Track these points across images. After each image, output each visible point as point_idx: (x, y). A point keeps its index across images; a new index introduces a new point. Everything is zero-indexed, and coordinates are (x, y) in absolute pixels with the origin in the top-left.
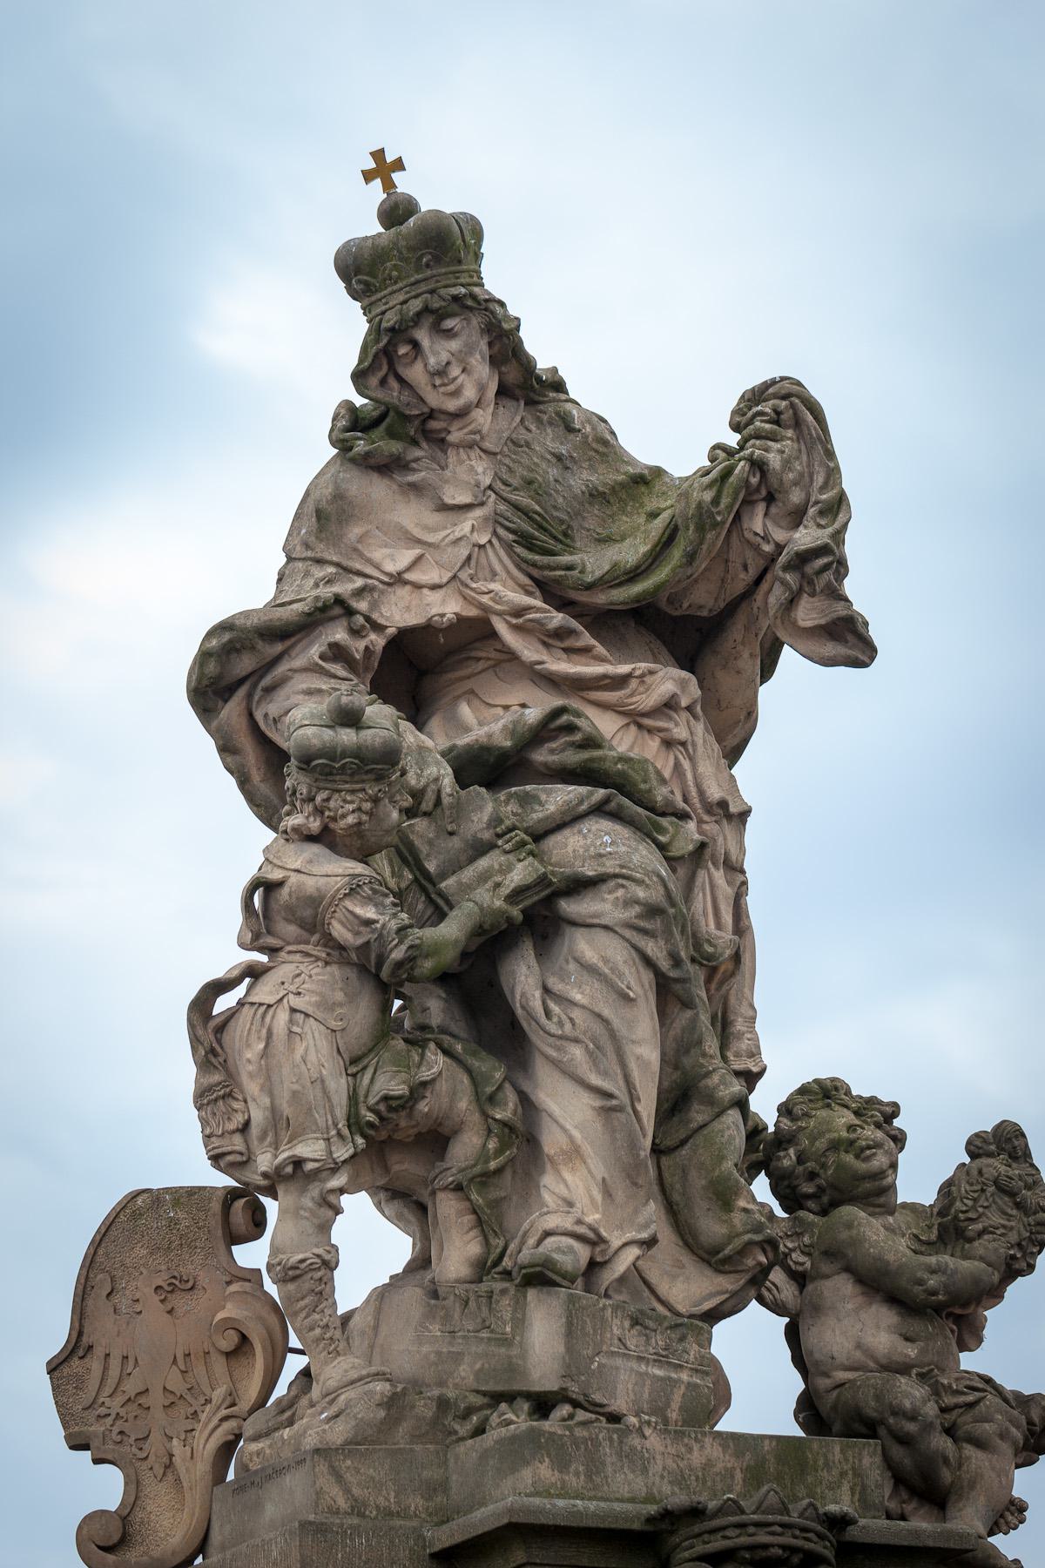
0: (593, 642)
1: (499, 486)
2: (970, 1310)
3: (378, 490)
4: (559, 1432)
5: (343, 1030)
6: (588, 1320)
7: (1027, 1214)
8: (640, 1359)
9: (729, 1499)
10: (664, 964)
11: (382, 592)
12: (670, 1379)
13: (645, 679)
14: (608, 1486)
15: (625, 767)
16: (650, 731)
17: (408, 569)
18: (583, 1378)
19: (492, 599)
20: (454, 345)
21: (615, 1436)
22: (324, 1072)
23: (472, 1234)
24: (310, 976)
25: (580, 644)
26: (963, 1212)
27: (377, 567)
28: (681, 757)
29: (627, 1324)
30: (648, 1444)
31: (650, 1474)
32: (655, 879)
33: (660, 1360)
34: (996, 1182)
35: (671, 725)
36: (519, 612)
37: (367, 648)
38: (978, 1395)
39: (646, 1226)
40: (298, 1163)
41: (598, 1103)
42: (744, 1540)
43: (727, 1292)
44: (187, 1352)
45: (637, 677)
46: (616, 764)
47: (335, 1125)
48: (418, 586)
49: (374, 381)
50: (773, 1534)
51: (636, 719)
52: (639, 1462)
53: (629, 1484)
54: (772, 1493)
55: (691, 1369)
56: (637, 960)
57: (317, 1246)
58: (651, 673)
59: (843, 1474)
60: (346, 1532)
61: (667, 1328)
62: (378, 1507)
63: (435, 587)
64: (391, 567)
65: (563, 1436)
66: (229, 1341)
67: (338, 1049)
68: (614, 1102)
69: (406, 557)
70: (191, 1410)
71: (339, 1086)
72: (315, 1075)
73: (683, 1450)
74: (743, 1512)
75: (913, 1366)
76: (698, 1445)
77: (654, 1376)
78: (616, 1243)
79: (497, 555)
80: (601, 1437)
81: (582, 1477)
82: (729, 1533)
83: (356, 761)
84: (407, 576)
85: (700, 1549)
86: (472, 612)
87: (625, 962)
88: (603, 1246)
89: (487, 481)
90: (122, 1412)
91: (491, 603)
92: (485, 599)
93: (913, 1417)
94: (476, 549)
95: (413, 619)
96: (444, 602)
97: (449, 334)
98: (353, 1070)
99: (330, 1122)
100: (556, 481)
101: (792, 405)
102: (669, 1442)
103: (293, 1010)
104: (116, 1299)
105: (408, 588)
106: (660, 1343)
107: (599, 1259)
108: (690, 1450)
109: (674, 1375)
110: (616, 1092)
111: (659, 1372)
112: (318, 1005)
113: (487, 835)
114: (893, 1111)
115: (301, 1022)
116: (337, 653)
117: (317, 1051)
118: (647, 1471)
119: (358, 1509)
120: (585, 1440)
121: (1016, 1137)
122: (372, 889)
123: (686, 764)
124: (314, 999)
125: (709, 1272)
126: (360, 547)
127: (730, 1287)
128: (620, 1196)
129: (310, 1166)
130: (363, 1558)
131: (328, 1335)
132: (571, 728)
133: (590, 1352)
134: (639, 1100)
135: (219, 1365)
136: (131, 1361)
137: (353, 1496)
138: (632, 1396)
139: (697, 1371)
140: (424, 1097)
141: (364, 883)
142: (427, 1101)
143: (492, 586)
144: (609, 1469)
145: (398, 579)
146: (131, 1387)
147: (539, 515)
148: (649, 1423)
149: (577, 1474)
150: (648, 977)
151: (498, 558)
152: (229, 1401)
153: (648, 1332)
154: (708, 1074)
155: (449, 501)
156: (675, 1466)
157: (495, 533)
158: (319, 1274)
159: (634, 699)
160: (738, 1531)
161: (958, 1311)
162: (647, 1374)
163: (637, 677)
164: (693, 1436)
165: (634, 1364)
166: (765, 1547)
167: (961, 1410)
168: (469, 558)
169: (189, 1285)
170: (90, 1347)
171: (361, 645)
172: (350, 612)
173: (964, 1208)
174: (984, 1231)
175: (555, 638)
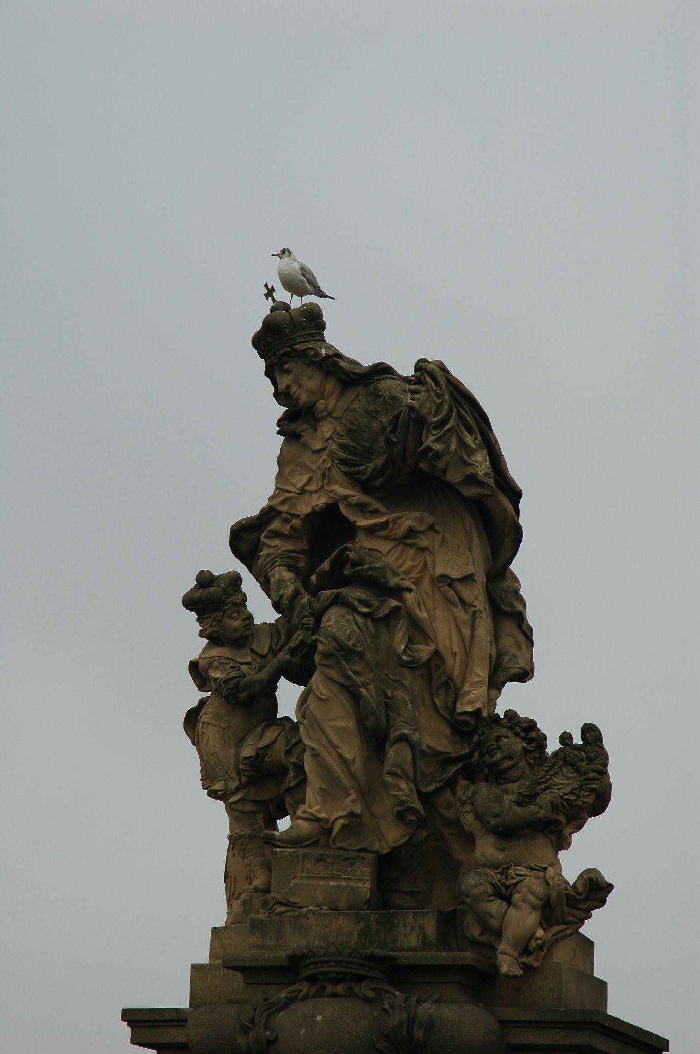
2: (560, 828)
5: (228, 727)
10: (341, 680)
13: (397, 522)
15: (372, 573)
16: (411, 545)
20: (290, 377)
24: (212, 705)
32: (329, 639)
35: (417, 541)
39: (344, 809)
42: (317, 970)
46: (368, 571)
48: (311, 493)
50: (330, 966)
54: (332, 946)
58: (400, 518)
59: (413, 929)
63: (316, 492)
64: (299, 485)
68: (316, 752)
69: (305, 478)
75: (502, 864)
78: (333, 818)
81: (273, 941)
82: (311, 967)
83: (201, 605)
85: (304, 975)
86: (331, 501)
89: (328, 435)
91: (334, 496)
92: (331, 495)
95: (309, 510)
96: (319, 498)
97: (288, 372)
103: (204, 722)
105: (308, 494)
116: (276, 534)
121: (589, 732)
122: (219, 663)
123: (429, 561)
126: (288, 477)
130: (220, 980)
131: (252, 868)
134: (338, 747)
145: (303, 491)
147: (353, 447)
150: (334, 687)
151: (336, 474)
153: (327, 864)
155: (314, 449)
156: (322, 931)
158: (240, 842)
163: (392, 522)
164: (333, 916)
166: (328, 973)
171: (288, 527)
172: (280, 513)
174: (547, 788)
175: (361, 508)
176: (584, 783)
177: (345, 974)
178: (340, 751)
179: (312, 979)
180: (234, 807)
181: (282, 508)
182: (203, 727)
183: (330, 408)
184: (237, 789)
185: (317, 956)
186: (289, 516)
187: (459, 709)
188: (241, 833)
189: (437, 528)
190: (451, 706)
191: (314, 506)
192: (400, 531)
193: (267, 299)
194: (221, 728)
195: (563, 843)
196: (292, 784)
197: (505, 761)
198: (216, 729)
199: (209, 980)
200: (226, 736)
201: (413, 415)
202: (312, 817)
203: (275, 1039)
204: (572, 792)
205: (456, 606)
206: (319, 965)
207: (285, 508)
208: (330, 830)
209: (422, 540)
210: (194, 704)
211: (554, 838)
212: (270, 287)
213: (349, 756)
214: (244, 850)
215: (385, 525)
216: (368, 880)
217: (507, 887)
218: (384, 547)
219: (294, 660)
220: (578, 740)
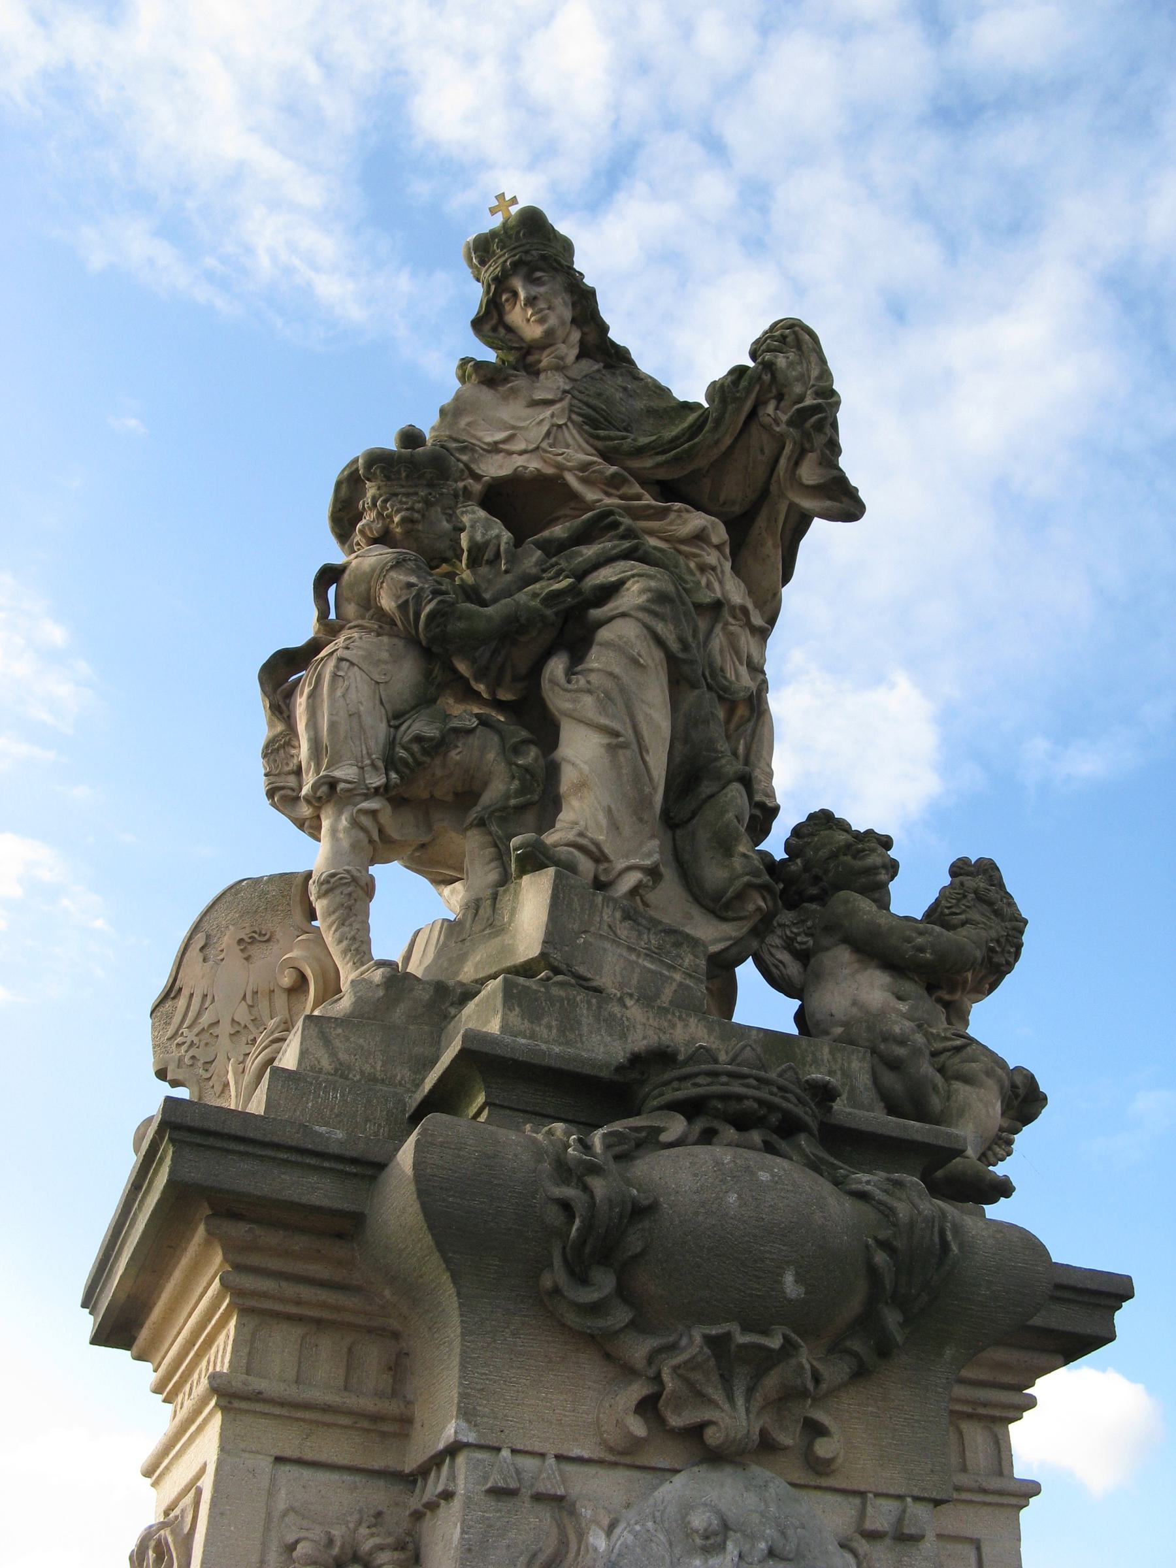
2: (957, 996)
4: (534, 987)
5: (386, 683)
6: (576, 900)
8: (631, 949)
9: (701, 1047)
10: (674, 646)
11: (482, 455)
12: (661, 974)
14: (582, 1043)
17: (504, 441)
18: (567, 949)
19: (565, 459)
22: (362, 708)
23: (493, 864)
26: (949, 908)
27: (480, 440)
28: (711, 577)
29: (618, 915)
30: (628, 1013)
31: (629, 1040)
33: (650, 955)
36: (584, 467)
39: (649, 855)
41: (606, 740)
42: (716, 1089)
43: (730, 938)
44: (255, 990)
45: (675, 511)
47: (369, 755)
48: (510, 453)
49: (487, 328)
50: (748, 1086)
52: (622, 1030)
53: (606, 1046)
54: (749, 1048)
55: (684, 972)
56: (648, 637)
57: (348, 865)
58: (687, 511)
60: (320, 1084)
61: (661, 931)
62: (362, 1073)
64: (489, 439)
65: (537, 991)
66: (287, 980)
67: (381, 700)
70: (251, 1037)
71: (379, 730)
72: (353, 710)
73: (666, 1024)
74: (716, 1061)
76: (683, 1023)
77: (645, 967)
78: (620, 865)
79: (571, 434)
80: (578, 999)
81: (554, 1031)
82: (700, 1080)
84: (502, 446)
85: (670, 1096)
86: (550, 471)
87: (637, 637)
88: (606, 865)
90: (196, 1040)
92: (559, 458)
93: (902, 1041)
94: (555, 428)
98: (397, 723)
99: (364, 752)
100: (621, 399)
101: (795, 333)
102: (651, 1015)
104: (207, 951)
105: (502, 454)
106: (653, 941)
107: (603, 878)
108: (674, 1026)
112: (365, 658)
113: (534, 571)
115: (346, 669)
117: (357, 691)
118: (626, 1038)
119: (341, 1070)
120: (561, 1000)
124: (361, 653)
125: (715, 922)
127: (734, 934)
128: (627, 831)
133: (576, 927)
135: (281, 1000)
136: (209, 999)
137: (338, 1059)
138: (619, 978)
139: (691, 976)
140: (457, 747)
141: (410, 560)
142: (459, 750)
144: (585, 1029)
145: (495, 448)
146: (205, 1020)
147: (605, 411)
149: (549, 1027)
150: (659, 655)
151: (572, 435)
152: (283, 1027)
153: (640, 928)
154: (717, 759)
157: (570, 419)
159: (673, 528)
160: (709, 1080)
162: (637, 963)
163: (675, 511)
166: (740, 1098)
167: (948, 1054)
168: (548, 434)
169: (265, 938)
170: (180, 989)
173: (949, 905)
175: (613, 484)
177: (771, 1107)
179: (691, 1108)
182: (337, 667)
186: (467, 473)
188: (355, 873)
191: (519, 467)
194: (372, 679)
196: (513, 802)
198: (365, 676)
199: (310, 1104)
202: (593, 848)
205: (741, 664)
207: (465, 458)
209: (709, 554)
219: (548, 612)
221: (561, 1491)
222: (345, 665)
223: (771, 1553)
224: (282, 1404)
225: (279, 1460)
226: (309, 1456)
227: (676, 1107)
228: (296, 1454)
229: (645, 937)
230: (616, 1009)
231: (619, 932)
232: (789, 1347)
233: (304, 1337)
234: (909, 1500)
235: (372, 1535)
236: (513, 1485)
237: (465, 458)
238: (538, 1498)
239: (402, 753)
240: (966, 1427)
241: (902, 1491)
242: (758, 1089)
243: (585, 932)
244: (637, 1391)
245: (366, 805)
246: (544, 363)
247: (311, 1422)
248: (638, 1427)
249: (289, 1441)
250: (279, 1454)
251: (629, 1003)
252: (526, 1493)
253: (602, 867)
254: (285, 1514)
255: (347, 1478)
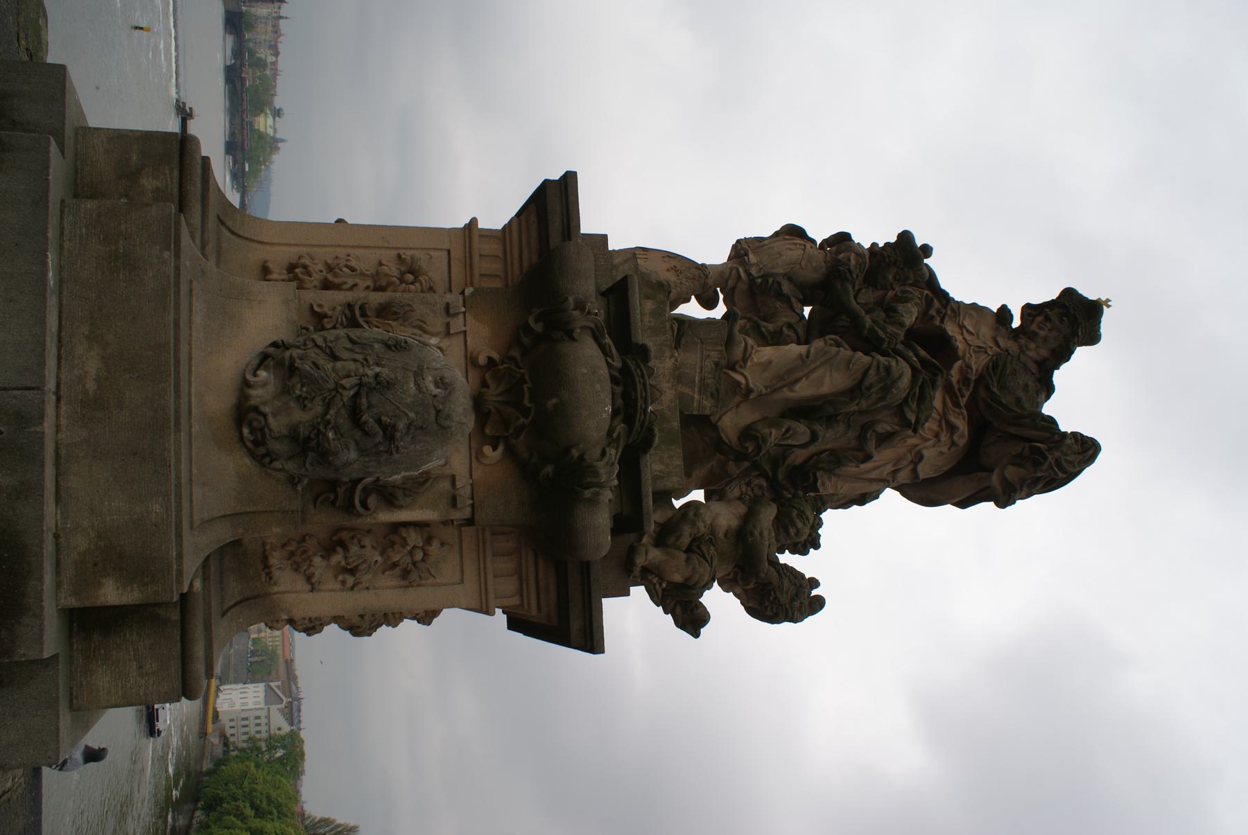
0: (967, 396)
1: (1010, 358)
2: (741, 583)
3: (991, 320)
5: (802, 268)
7: (789, 603)
8: (701, 368)
10: (867, 382)
12: (695, 386)
16: (940, 426)
20: (1057, 323)
21: (668, 343)
22: (784, 257)
25: (965, 392)
27: (964, 319)
28: (933, 441)
29: (716, 359)
30: (667, 360)
33: (702, 380)
34: (801, 586)
35: (945, 433)
36: (969, 367)
37: (934, 316)
38: (710, 560)
39: (755, 385)
40: (746, 254)
43: (731, 443)
47: (765, 266)
48: (962, 334)
49: (1029, 311)
51: (944, 416)
55: (700, 401)
58: (964, 418)
63: (965, 339)
64: (965, 323)
73: (667, 378)
74: (649, 378)
77: (695, 377)
78: (745, 373)
79: (986, 358)
80: (667, 335)
82: (638, 371)
86: (960, 353)
88: (743, 365)
92: (968, 355)
95: (950, 333)
96: (961, 342)
97: (1061, 321)
103: (805, 245)
105: (960, 331)
107: (737, 367)
108: (668, 382)
109: (696, 389)
110: (810, 359)
111: (697, 379)
114: (817, 546)
121: (819, 604)
123: (930, 443)
129: (746, 258)
132: (936, 375)
134: (807, 379)
140: (782, 304)
143: (974, 357)
145: (962, 327)
148: (676, 361)
149: (650, 322)
151: (984, 359)
157: (993, 356)
158: (702, 275)
159: (951, 413)
161: (739, 577)
165: (698, 365)
168: (980, 347)
171: (934, 314)
172: (945, 307)
175: (965, 380)
176: (784, 607)
178: (804, 379)
179: (625, 370)
180: (734, 271)
181: (949, 308)
182: (800, 244)
183: (1028, 352)
184: (749, 275)
185: (649, 378)
186: (942, 315)
187: (819, 474)
189: (953, 449)
190: (820, 465)
192: (952, 419)
193: (1110, 306)
195: (726, 587)
196: (763, 329)
197: (795, 531)
200: (794, 266)
201: (1056, 436)
202: (747, 354)
203: (573, 339)
204: (776, 597)
205: (894, 466)
206: (642, 381)
207: (949, 312)
208: (734, 369)
209: (946, 436)
210: (810, 234)
211: (731, 576)
212: (1109, 303)
213: (797, 387)
214: (694, 278)
215: (957, 405)
216: (699, 410)
217: (699, 547)
218: (937, 403)
220: (814, 592)
221: (452, 331)
222: (803, 247)
223: (438, 412)
224: (470, 248)
225: (449, 252)
226: (452, 262)
227: (625, 363)
228: (452, 257)
229: (710, 376)
230: (668, 354)
231: (707, 360)
232: (525, 412)
233: (497, 257)
234: (471, 502)
235: (425, 281)
236: (452, 311)
237: (949, 312)
238: (448, 325)
239: (771, 280)
240: (515, 577)
241: (475, 498)
242: (642, 397)
243: (702, 342)
244: (496, 356)
245: (741, 270)
246: (1020, 340)
247: (466, 261)
248: (482, 360)
249: (457, 254)
250: (451, 250)
251: (673, 360)
252: (449, 319)
253: (741, 363)
254: (429, 255)
255: (447, 279)
